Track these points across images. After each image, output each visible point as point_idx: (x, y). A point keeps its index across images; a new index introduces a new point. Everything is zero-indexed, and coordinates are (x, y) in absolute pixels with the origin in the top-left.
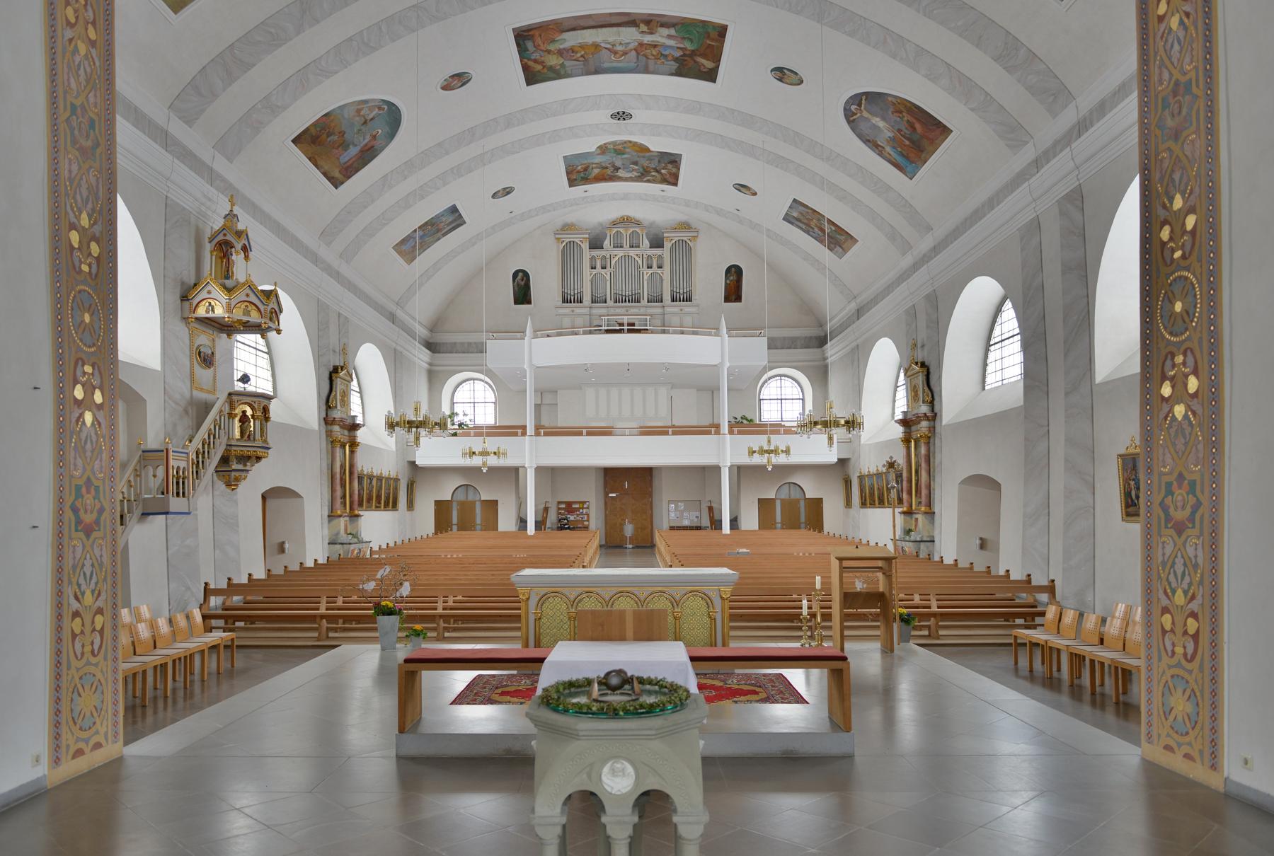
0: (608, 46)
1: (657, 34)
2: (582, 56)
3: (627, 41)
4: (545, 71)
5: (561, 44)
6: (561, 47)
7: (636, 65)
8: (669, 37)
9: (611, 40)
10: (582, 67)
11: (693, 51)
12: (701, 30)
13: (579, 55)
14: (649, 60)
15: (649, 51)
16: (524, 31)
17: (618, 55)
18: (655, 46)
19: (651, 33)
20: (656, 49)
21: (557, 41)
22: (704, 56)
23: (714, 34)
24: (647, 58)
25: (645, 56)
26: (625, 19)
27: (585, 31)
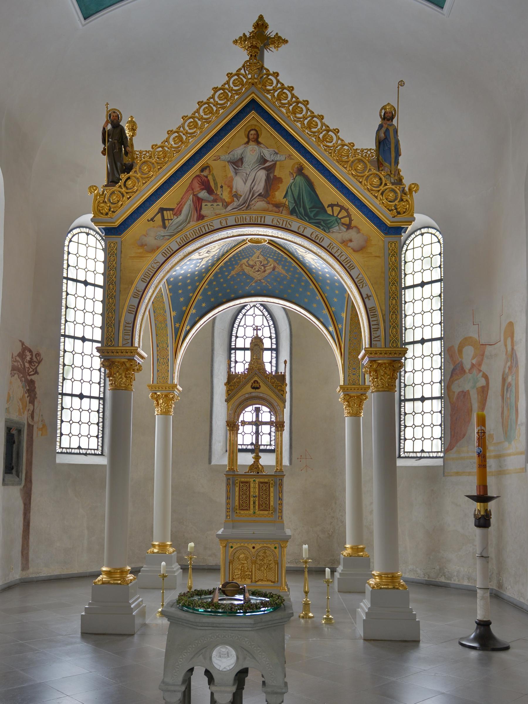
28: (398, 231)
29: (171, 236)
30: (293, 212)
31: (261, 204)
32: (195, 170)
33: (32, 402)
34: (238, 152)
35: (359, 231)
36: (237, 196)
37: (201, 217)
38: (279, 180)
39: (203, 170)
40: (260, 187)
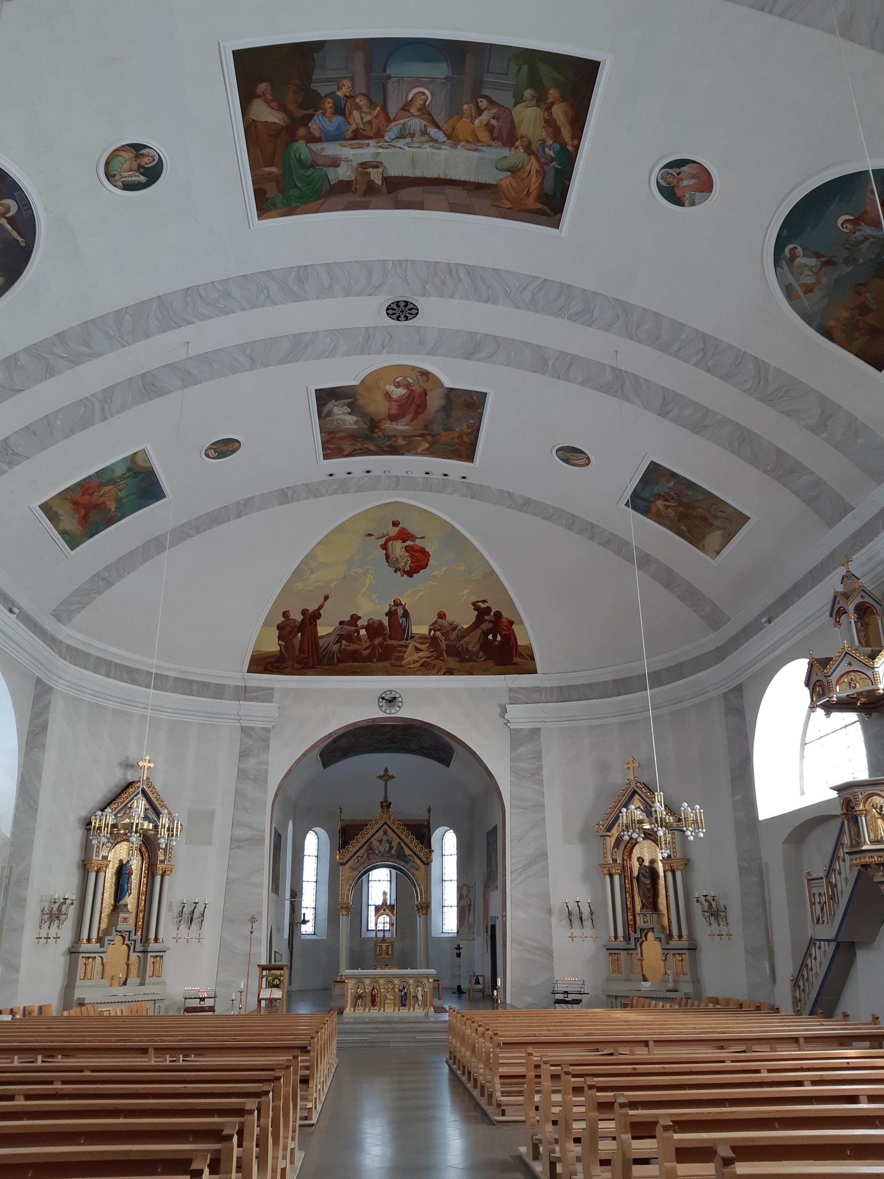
0: (433, 131)
1: (355, 164)
2: (480, 112)
3: (400, 143)
4: (553, 94)
5: (506, 157)
6: (505, 152)
7: (388, 71)
8: (335, 163)
9: (427, 149)
10: (487, 78)
11: (294, 139)
12: (292, 192)
13: (485, 117)
14: (364, 92)
15: (367, 118)
16: (547, 215)
17: (419, 102)
18: (357, 135)
19: (364, 165)
20: (354, 127)
21: (508, 170)
22: (275, 132)
23: (271, 190)
24: (367, 96)
25: (372, 104)
26: (405, 194)
27: (463, 179)
28: (428, 864)
29: (361, 865)
30: (397, 857)
31: (388, 855)
32: (368, 844)
33: (293, 913)
34: (380, 838)
35: (416, 863)
36: (380, 852)
37: (369, 859)
38: (393, 847)
39: (370, 843)
40: (387, 849)
